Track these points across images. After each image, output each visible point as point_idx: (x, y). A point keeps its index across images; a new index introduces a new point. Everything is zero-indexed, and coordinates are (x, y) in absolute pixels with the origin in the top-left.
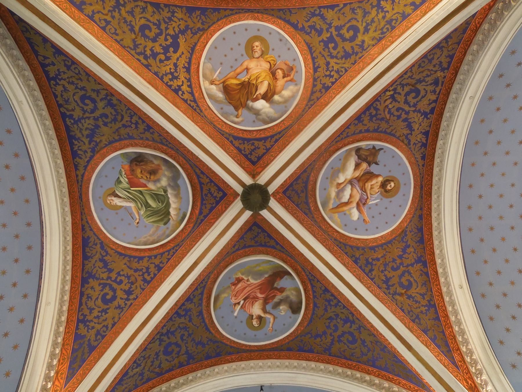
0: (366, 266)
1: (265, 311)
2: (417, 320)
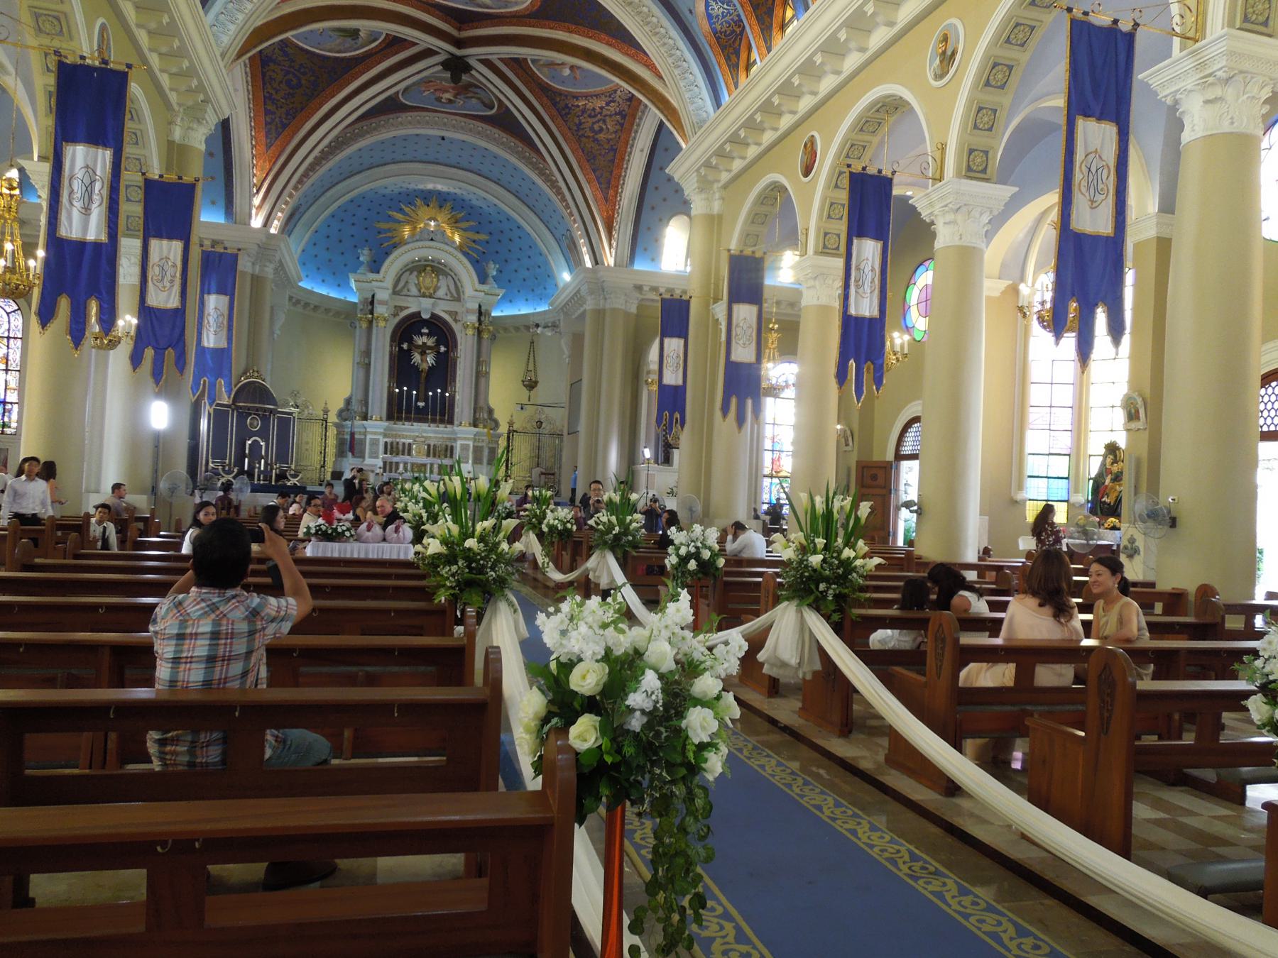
0: (563, 109)
1: (455, 96)
2: (592, 161)
